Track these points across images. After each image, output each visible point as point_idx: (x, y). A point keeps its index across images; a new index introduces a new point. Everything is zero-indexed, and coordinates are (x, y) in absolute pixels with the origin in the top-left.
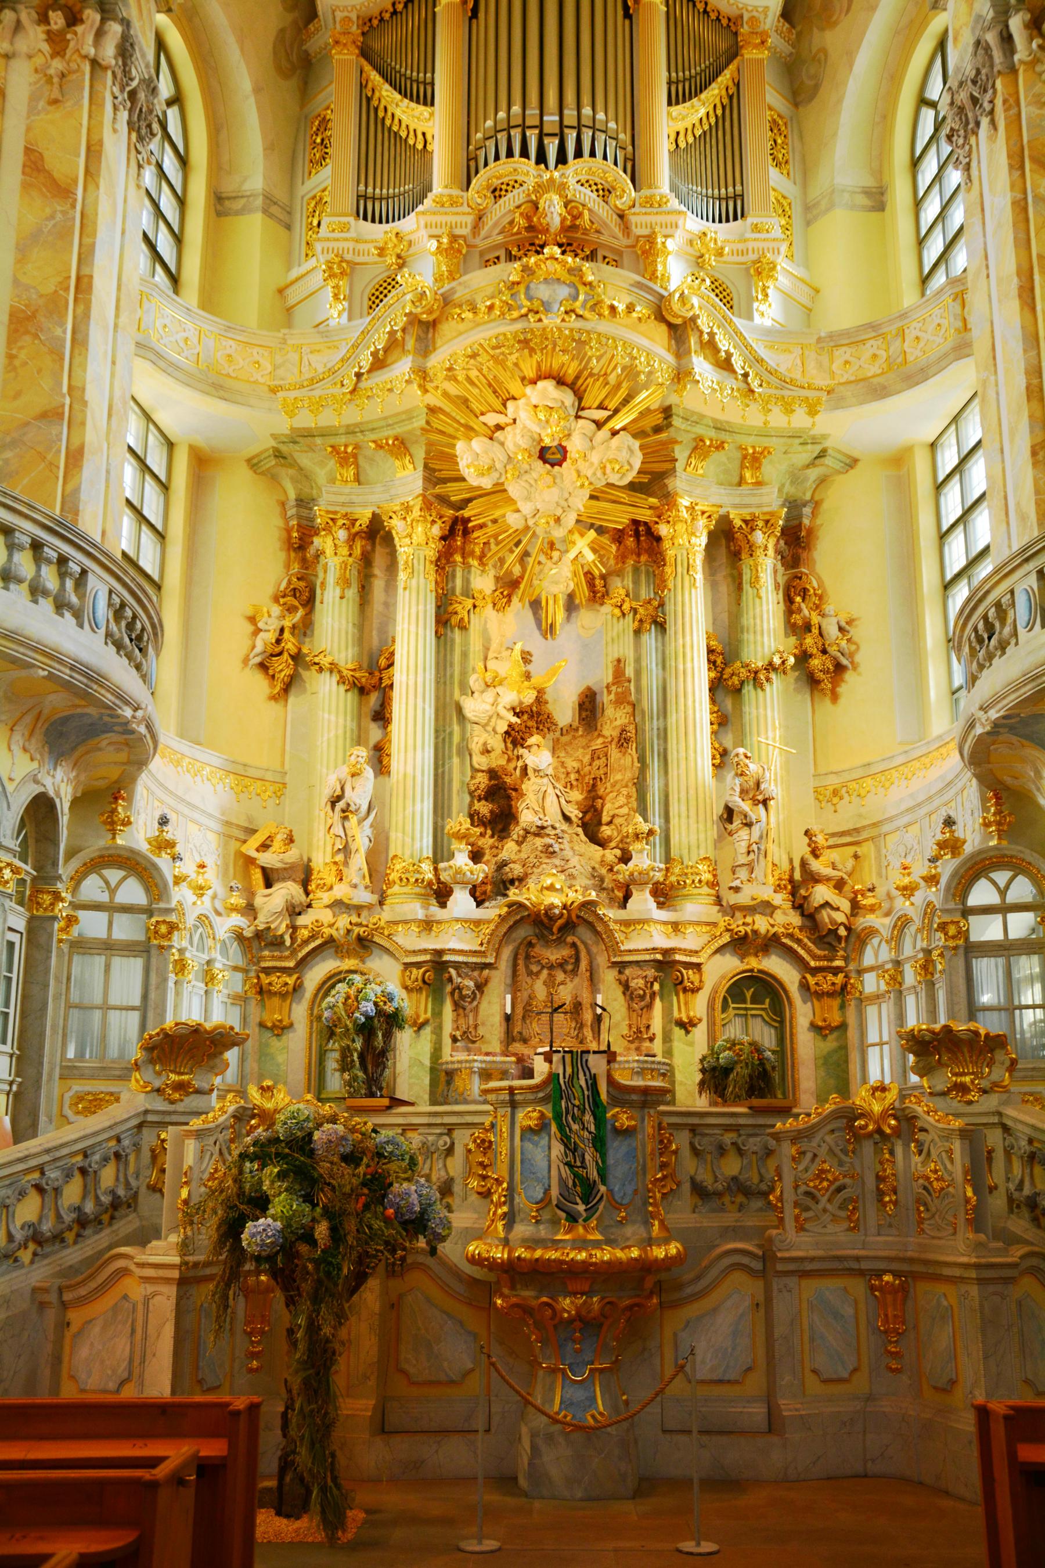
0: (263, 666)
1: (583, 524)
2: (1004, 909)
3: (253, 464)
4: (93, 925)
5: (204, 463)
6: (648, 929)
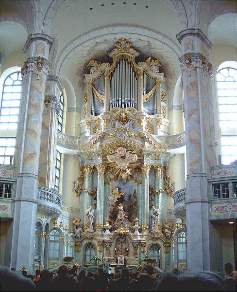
0: (76, 191)
1: (129, 168)
2: (183, 237)
3: (74, 156)
4: (52, 238)
5: (66, 156)
6: (139, 237)
